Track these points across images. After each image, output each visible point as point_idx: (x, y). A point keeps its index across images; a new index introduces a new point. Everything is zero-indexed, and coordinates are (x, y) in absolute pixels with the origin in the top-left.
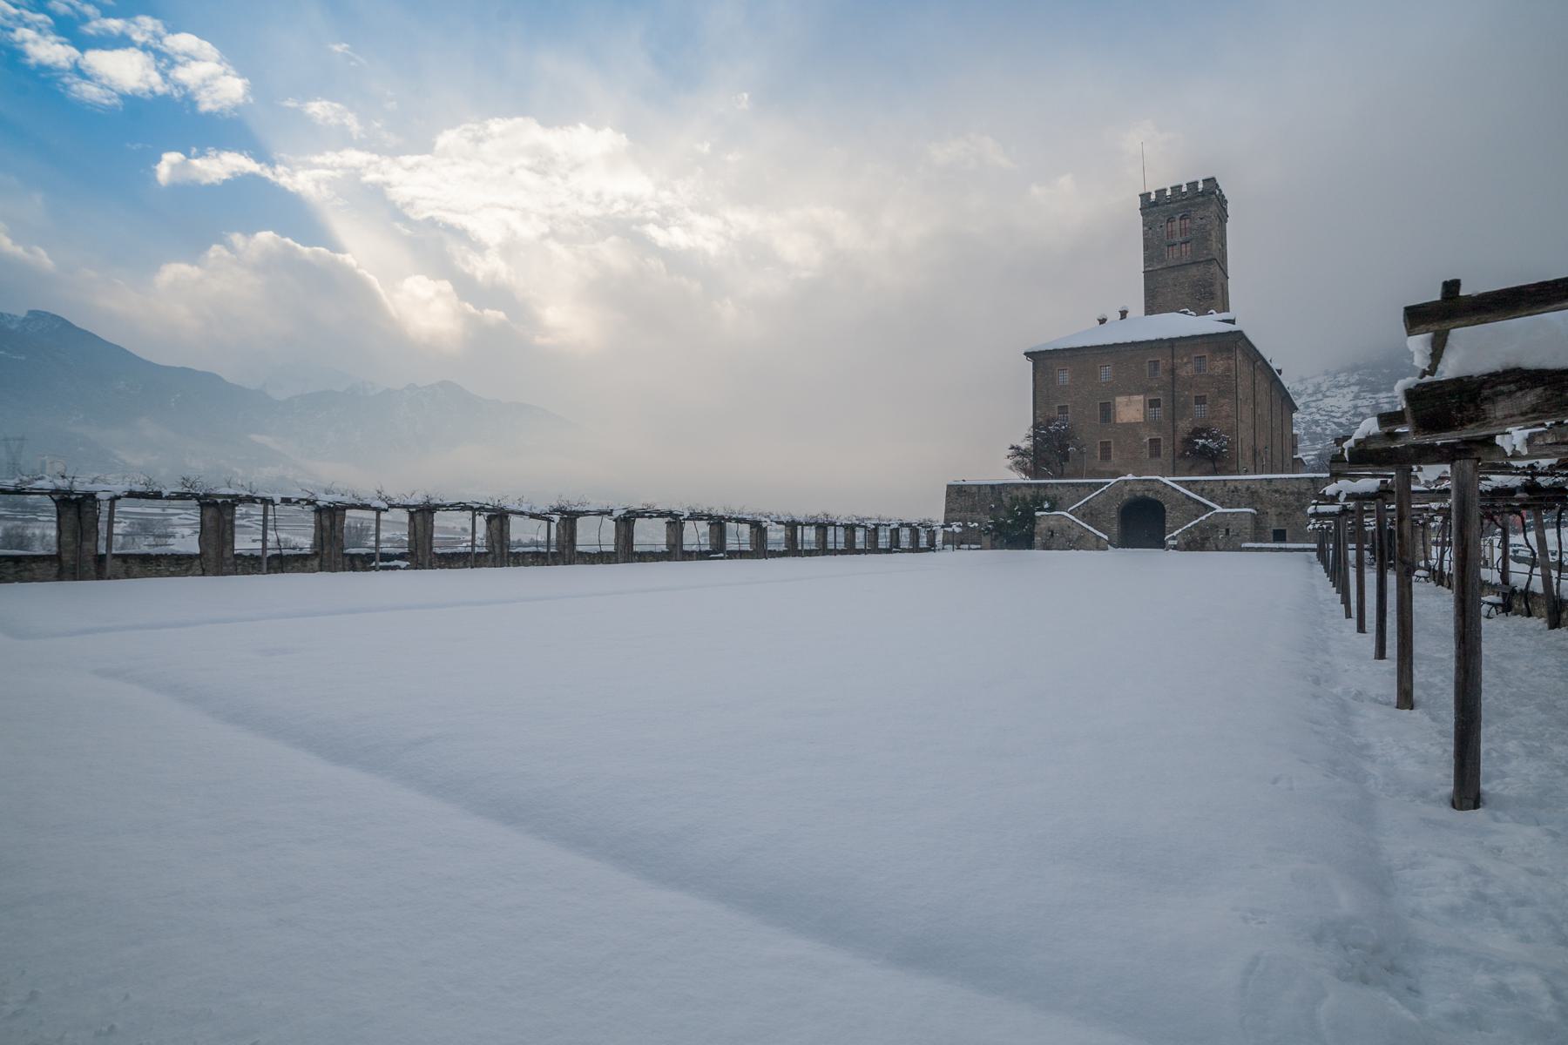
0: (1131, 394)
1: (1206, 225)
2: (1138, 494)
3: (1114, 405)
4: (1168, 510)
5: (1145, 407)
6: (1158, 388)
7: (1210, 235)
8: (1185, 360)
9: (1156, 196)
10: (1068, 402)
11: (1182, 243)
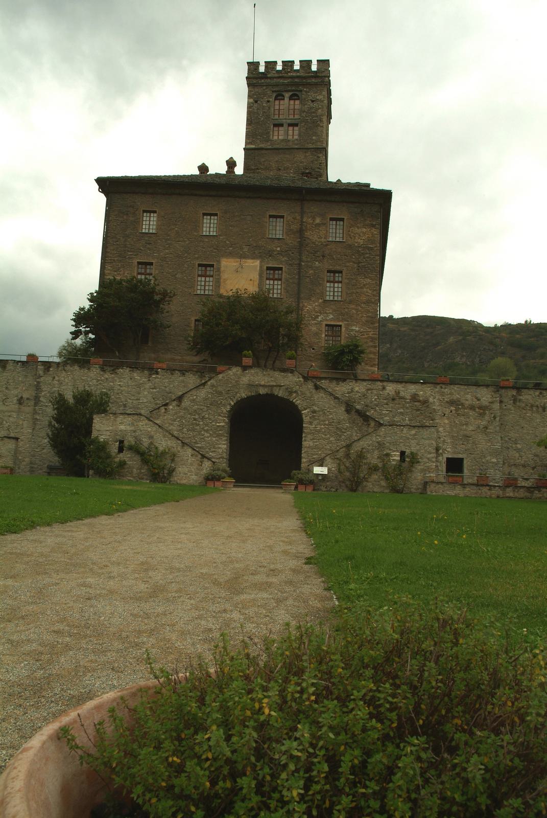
1: (317, 110)
3: (219, 270)
4: (306, 419)
5: (261, 276)
6: (280, 253)
8: (318, 221)
9: (266, 67)
11: (290, 125)
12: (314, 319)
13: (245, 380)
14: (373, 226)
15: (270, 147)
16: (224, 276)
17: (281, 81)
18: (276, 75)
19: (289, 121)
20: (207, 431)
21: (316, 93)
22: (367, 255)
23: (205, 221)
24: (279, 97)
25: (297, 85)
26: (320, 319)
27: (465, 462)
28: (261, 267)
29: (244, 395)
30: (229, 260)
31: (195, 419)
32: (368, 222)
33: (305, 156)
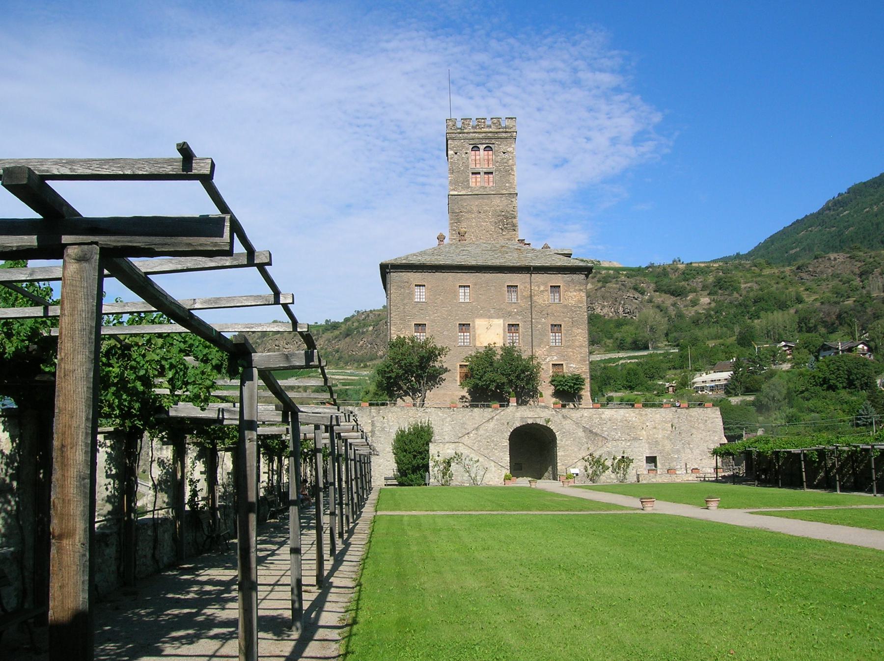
0: (490, 317)
2: (530, 421)
3: (474, 327)
4: (558, 438)
6: (516, 313)
7: (512, 170)
8: (542, 288)
10: (427, 320)
11: (485, 173)
12: (544, 361)
13: (518, 415)
14: (581, 290)
15: (470, 193)
16: (478, 332)
17: (477, 135)
18: (472, 131)
19: (485, 170)
20: (496, 449)
21: (507, 145)
22: (578, 312)
23: (460, 291)
24: (475, 148)
25: (490, 138)
26: (548, 360)
27: (658, 458)
28: (504, 324)
29: (518, 425)
30: (481, 320)
31: (488, 442)
32: (577, 288)
33: (501, 200)
